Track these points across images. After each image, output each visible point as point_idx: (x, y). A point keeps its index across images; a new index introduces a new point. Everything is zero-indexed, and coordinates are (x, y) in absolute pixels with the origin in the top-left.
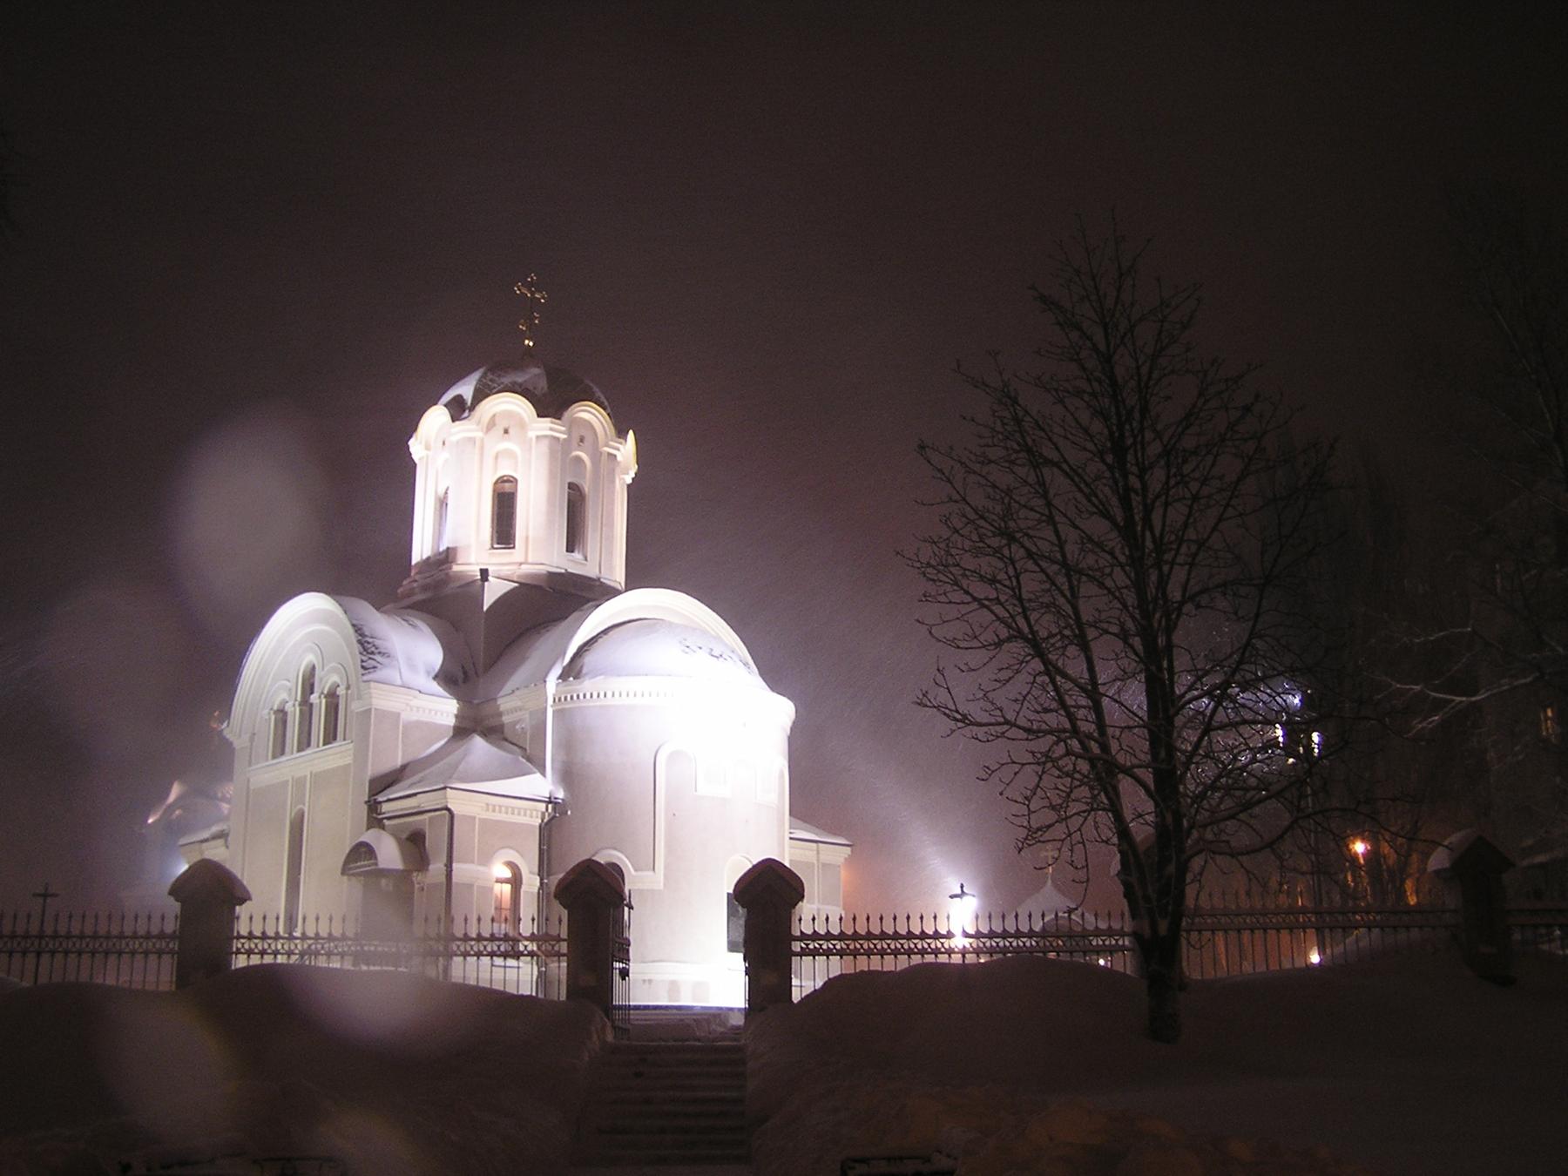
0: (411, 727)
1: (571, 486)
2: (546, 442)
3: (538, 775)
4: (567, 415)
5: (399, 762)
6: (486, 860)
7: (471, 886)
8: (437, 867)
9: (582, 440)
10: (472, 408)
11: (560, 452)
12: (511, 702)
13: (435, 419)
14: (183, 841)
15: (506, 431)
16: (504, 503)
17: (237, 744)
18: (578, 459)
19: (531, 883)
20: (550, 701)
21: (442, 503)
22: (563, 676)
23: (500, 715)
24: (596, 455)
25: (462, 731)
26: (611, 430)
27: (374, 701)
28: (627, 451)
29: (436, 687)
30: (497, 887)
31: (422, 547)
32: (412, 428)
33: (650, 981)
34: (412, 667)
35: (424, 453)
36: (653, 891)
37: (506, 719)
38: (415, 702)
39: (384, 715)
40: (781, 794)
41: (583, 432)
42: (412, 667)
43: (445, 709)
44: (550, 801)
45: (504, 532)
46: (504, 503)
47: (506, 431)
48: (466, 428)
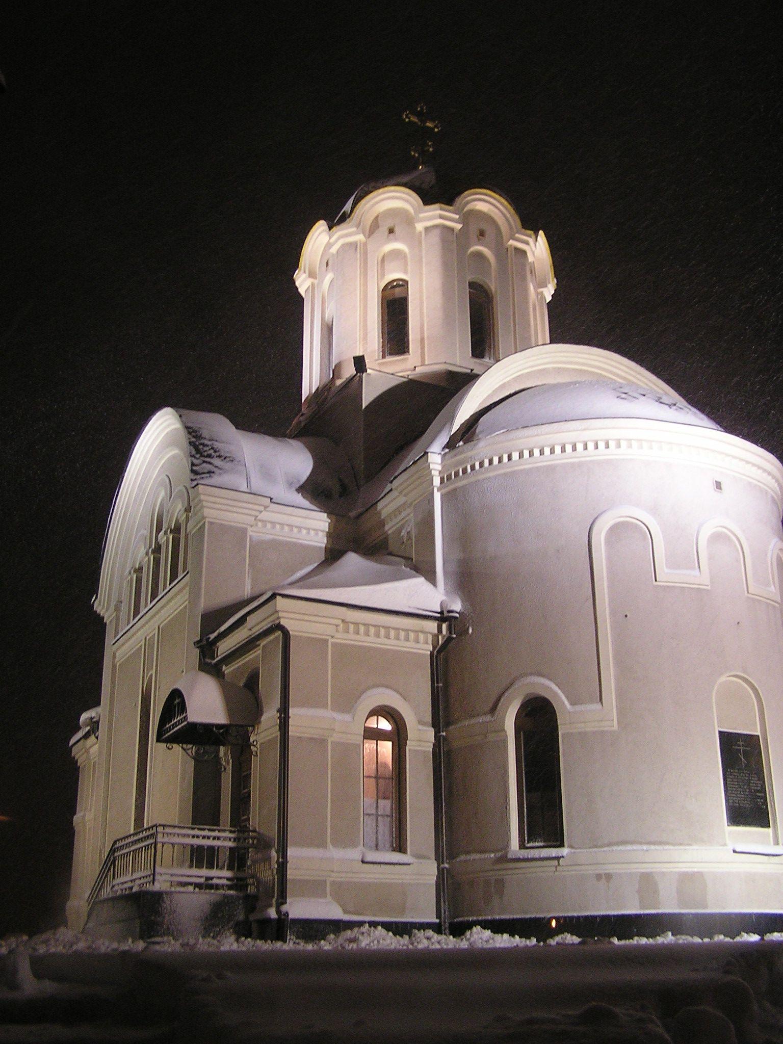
0: (260, 548)
1: (472, 285)
2: (437, 232)
3: (421, 580)
4: (459, 201)
5: (247, 592)
6: (346, 702)
7: (322, 742)
8: (270, 716)
9: (482, 233)
10: (349, 216)
11: (454, 245)
12: (393, 505)
13: (319, 240)
14: (71, 743)
15: (391, 231)
16: (395, 308)
17: (108, 616)
18: (479, 255)
19: (421, 738)
20: (437, 481)
21: (328, 329)
22: (451, 445)
23: (382, 524)
24: (502, 251)
25: (333, 555)
26: (515, 221)
27: (206, 512)
28: (538, 249)
29: (299, 499)
30: (370, 745)
31: (311, 378)
33: (609, 877)
37: (390, 528)
38: (265, 515)
39: (225, 529)
41: (484, 226)
42: (267, 474)
43: (313, 526)
44: (443, 617)
45: (396, 336)
46: (395, 308)
47: (391, 231)
48: (347, 234)
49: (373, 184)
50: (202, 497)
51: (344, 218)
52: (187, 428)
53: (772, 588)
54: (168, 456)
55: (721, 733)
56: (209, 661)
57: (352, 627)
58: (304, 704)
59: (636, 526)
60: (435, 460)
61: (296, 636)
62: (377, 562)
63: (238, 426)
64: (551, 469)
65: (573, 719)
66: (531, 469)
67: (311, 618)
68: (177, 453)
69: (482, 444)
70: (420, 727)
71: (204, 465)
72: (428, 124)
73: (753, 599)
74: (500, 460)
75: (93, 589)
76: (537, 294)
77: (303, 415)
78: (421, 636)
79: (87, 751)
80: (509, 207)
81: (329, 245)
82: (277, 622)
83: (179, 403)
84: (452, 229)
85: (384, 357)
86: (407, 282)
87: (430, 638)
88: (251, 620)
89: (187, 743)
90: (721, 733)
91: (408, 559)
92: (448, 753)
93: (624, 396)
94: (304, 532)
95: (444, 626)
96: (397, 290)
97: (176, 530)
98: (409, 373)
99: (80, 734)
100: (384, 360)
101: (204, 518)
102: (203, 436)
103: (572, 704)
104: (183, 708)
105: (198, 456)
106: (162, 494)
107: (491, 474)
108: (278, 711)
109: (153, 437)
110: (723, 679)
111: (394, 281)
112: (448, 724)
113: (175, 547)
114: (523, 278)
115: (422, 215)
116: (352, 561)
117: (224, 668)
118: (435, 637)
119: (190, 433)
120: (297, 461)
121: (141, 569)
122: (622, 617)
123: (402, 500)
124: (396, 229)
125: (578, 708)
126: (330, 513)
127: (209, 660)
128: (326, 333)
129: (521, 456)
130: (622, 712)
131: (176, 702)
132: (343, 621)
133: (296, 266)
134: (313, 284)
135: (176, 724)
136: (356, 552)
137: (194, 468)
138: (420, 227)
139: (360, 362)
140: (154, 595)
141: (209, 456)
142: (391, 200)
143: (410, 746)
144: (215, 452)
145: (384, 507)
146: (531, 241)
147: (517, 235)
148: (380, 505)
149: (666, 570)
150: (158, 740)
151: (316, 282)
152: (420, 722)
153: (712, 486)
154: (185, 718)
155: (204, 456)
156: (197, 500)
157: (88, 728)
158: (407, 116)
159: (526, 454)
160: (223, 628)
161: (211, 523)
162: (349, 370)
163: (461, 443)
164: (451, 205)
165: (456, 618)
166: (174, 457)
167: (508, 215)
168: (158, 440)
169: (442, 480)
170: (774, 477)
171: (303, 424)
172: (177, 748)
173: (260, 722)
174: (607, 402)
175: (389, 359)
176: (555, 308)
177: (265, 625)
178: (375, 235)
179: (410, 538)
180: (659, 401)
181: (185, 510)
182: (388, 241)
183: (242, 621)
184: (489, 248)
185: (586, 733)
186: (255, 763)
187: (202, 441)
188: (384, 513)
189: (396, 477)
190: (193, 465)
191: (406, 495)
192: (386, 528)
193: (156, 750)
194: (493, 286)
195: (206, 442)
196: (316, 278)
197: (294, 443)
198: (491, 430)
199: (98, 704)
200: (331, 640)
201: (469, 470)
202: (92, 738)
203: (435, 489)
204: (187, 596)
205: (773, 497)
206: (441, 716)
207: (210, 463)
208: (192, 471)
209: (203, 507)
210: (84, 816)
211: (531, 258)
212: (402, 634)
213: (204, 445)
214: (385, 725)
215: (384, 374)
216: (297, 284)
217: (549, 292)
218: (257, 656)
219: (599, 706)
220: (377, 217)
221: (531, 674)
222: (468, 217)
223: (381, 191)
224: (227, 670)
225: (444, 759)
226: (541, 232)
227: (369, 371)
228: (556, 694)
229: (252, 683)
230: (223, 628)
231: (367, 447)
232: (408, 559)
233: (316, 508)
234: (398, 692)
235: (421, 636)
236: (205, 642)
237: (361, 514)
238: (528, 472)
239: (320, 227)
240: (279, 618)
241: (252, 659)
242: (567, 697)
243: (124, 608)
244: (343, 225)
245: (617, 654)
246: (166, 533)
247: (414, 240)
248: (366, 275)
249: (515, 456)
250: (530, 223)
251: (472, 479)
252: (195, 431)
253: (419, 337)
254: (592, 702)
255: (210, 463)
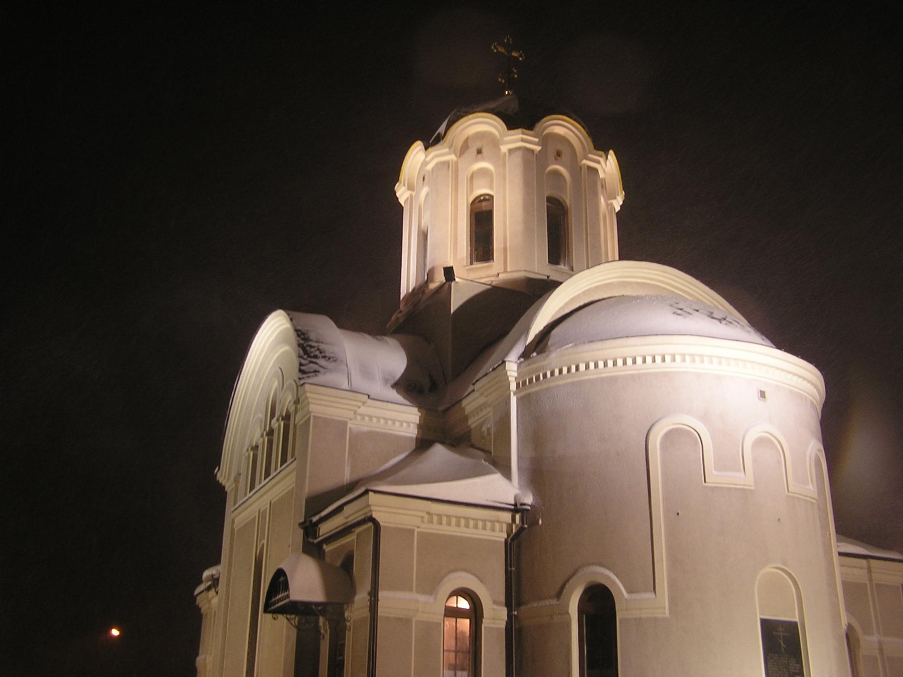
0: (358, 439)
1: (550, 200)
2: (519, 154)
4: (539, 126)
5: (347, 476)
6: (430, 585)
7: (407, 621)
8: (362, 597)
9: (559, 154)
11: (535, 165)
12: (475, 402)
13: (417, 158)
14: (196, 592)
15: (479, 152)
16: (481, 219)
17: (229, 486)
18: (556, 173)
19: (496, 616)
20: (513, 387)
21: (424, 236)
22: (526, 355)
23: (466, 419)
24: (576, 169)
25: (423, 444)
26: (588, 142)
27: (312, 407)
28: (608, 166)
29: (394, 395)
30: (449, 623)
31: (409, 279)
32: (394, 174)
34: (366, 373)
35: (407, 194)
36: (655, 620)
37: (473, 422)
40: (821, 489)
41: (559, 147)
42: (366, 373)
43: (405, 419)
44: (516, 509)
46: (481, 219)
47: (479, 152)
48: (441, 154)
49: (464, 109)
50: (308, 395)
51: (438, 140)
52: (296, 331)
53: (811, 487)
54: (281, 351)
55: (764, 622)
56: (311, 540)
57: (435, 518)
58: (391, 588)
59: (688, 432)
60: (512, 368)
61: (385, 527)
62: (462, 453)
63: (341, 326)
64: (613, 380)
65: (629, 605)
66: (596, 379)
67: (400, 511)
68: (288, 350)
69: (553, 356)
70: (495, 607)
71: (311, 365)
72: (513, 54)
73: (793, 497)
74: (569, 370)
75: (217, 461)
76: (607, 205)
77: (401, 312)
78: (497, 525)
79: (209, 601)
80: (583, 130)
81: (425, 163)
82: (369, 515)
83: (291, 307)
84: (532, 151)
85: (471, 263)
86: (492, 197)
87: (505, 527)
88: (348, 510)
89: (291, 614)
90: (764, 622)
91: (487, 452)
92: (519, 631)
93: (679, 312)
94: (398, 424)
95: (518, 516)
96: (484, 204)
97: (287, 418)
98: (493, 279)
99: (202, 587)
100: (472, 267)
101: (309, 412)
102: (311, 338)
103: (630, 592)
104: (286, 587)
105: (305, 357)
106: (276, 384)
107: (561, 383)
108: (370, 594)
109: (269, 334)
110: (768, 569)
111: (481, 195)
112: (519, 604)
113: (286, 433)
114: (595, 194)
115: (506, 139)
116: (439, 453)
117: (325, 546)
118: (510, 526)
119: (299, 336)
120: (392, 359)
121: (257, 447)
122: (674, 515)
123: (482, 400)
124: (484, 150)
125: (634, 596)
126: (420, 408)
127: (312, 546)
128: (422, 239)
129: (587, 367)
130: (672, 599)
131: (280, 581)
132: (428, 513)
133: (396, 178)
134: (411, 196)
135: (280, 600)
136: (443, 443)
137: (302, 368)
138: (504, 149)
139: (449, 273)
140: (267, 474)
141: (316, 357)
142: (480, 125)
143: (486, 623)
144: (321, 353)
145: (469, 404)
146: (602, 160)
147: (590, 156)
148: (464, 403)
149: (714, 472)
150: (266, 611)
151: (414, 194)
152: (495, 602)
153: (756, 395)
154: (288, 596)
155: (309, 356)
156: (303, 397)
157: (209, 583)
158: (495, 47)
159: (592, 365)
160: (323, 514)
161: (314, 417)
162: (440, 278)
163: (535, 354)
164: (532, 130)
165: (527, 510)
166: (286, 351)
167: (583, 139)
168: (272, 336)
169: (518, 385)
170: (812, 384)
171: (401, 321)
172: (282, 618)
173: (353, 602)
174: (665, 319)
175: (477, 265)
176: (623, 217)
177: (359, 517)
178: (466, 155)
179: (489, 434)
180: (711, 316)
181: (295, 403)
182: (477, 160)
183: (340, 509)
184: (563, 166)
185: (640, 619)
186: (349, 637)
187: (310, 343)
188: (468, 410)
189: (477, 381)
190: (301, 364)
191: (486, 396)
192: (470, 422)
193: (265, 619)
194: (568, 200)
195: (313, 344)
196: (413, 190)
197: (392, 342)
198: (563, 343)
199: (217, 561)
200: (417, 530)
201: (541, 378)
202: (212, 592)
203: (512, 394)
204: (294, 479)
205: (812, 403)
206: (514, 597)
207: (316, 363)
208: (301, 371)
209: (308, 403)
210: (205, 659)
211: (602, 175)
212: (480, 524)
213: (311, 347)
214: (464, 604)
215: (471, 280)
216: (398, 195)
217: (617, 203)
218: (353, 540)
219: (652, 595)
220: (467, 140)
221: (593, 564)
222: (545, 140)
223: (471, 116)
224: (327, 548)
225: (514, 635)
226: (611, 152)
227: (457, 279)
228: (614, 583)
229: (348, 564)
230: (323, 514)
231: (454, 347)
232: (487, 452)
233: (406, 402)
234: (474, 574)
235: (497, 525)
236: (308, 524)
237: (449, 408)
238: (592, 382)
239: (417, 148)
240: (371, 511)
241: (347, 543)
242: (624, 586)
243: (242, 479)
244: (438, 146)
245: (670, 548)
246: (278, 420)
247: (499, 160)
248: (456, 192)
249: (582, 367)
250: (601, 145)
251: (545, 386)
252: (303, 334)
253: (502, 246)
254: (646, 591)
255: (316, 363)
